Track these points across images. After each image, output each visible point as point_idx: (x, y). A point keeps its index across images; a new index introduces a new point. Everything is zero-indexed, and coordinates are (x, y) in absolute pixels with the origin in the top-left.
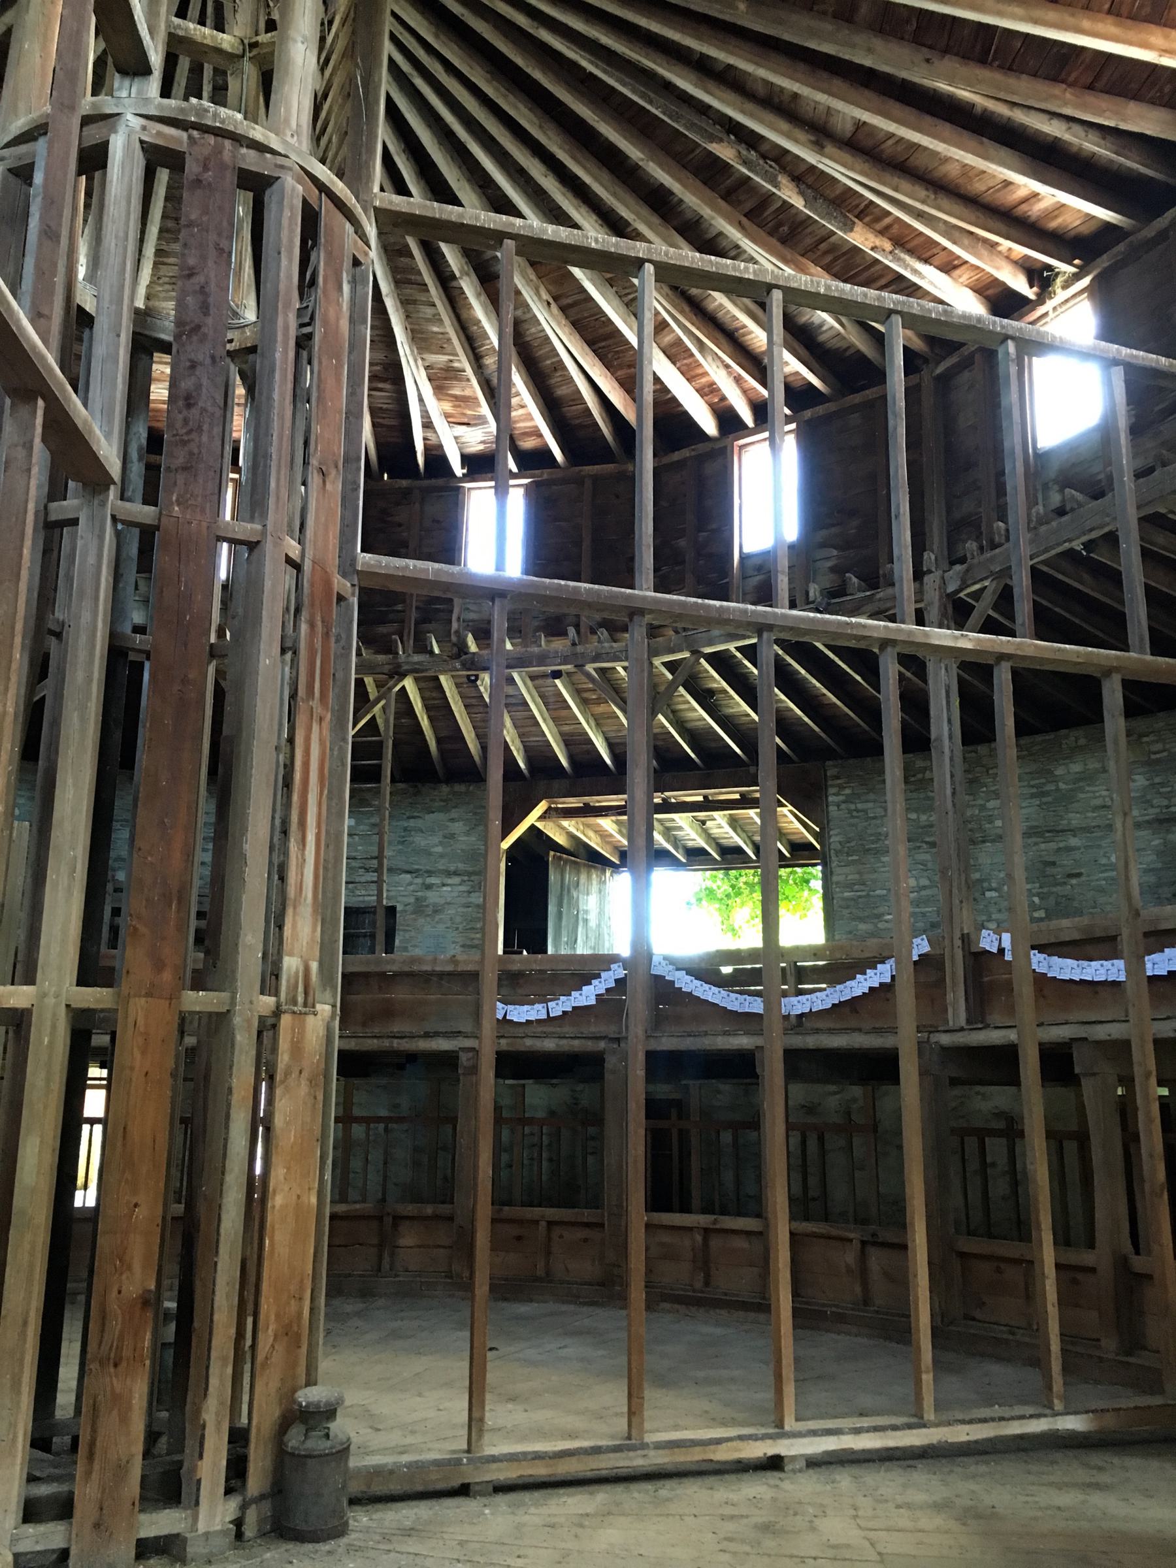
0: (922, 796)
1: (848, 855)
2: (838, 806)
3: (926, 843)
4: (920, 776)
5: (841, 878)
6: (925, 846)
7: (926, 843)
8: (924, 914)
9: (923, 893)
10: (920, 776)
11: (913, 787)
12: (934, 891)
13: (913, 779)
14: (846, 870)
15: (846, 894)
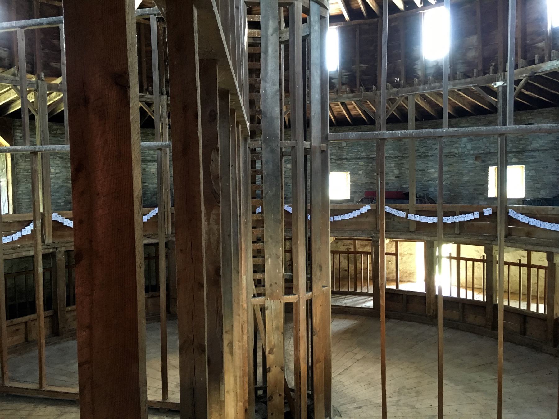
0: (56, 139)
1: (26, 158)
2: (21, 138)
3: (58, 157)
4: (55, 132)
5: (23, 167)
6: (57, 158)
7: (58, 157)
8: (57, 183)
9: (57, 175)
10: (55, 132)
11: (53, 135)
12: (61, 174)
13: (52, 132)
14: (25, 164)
15: (25, 173)
